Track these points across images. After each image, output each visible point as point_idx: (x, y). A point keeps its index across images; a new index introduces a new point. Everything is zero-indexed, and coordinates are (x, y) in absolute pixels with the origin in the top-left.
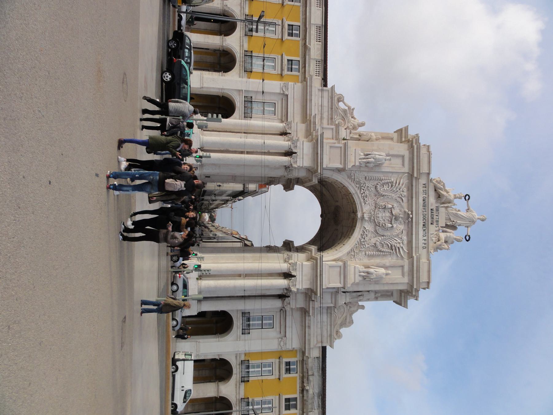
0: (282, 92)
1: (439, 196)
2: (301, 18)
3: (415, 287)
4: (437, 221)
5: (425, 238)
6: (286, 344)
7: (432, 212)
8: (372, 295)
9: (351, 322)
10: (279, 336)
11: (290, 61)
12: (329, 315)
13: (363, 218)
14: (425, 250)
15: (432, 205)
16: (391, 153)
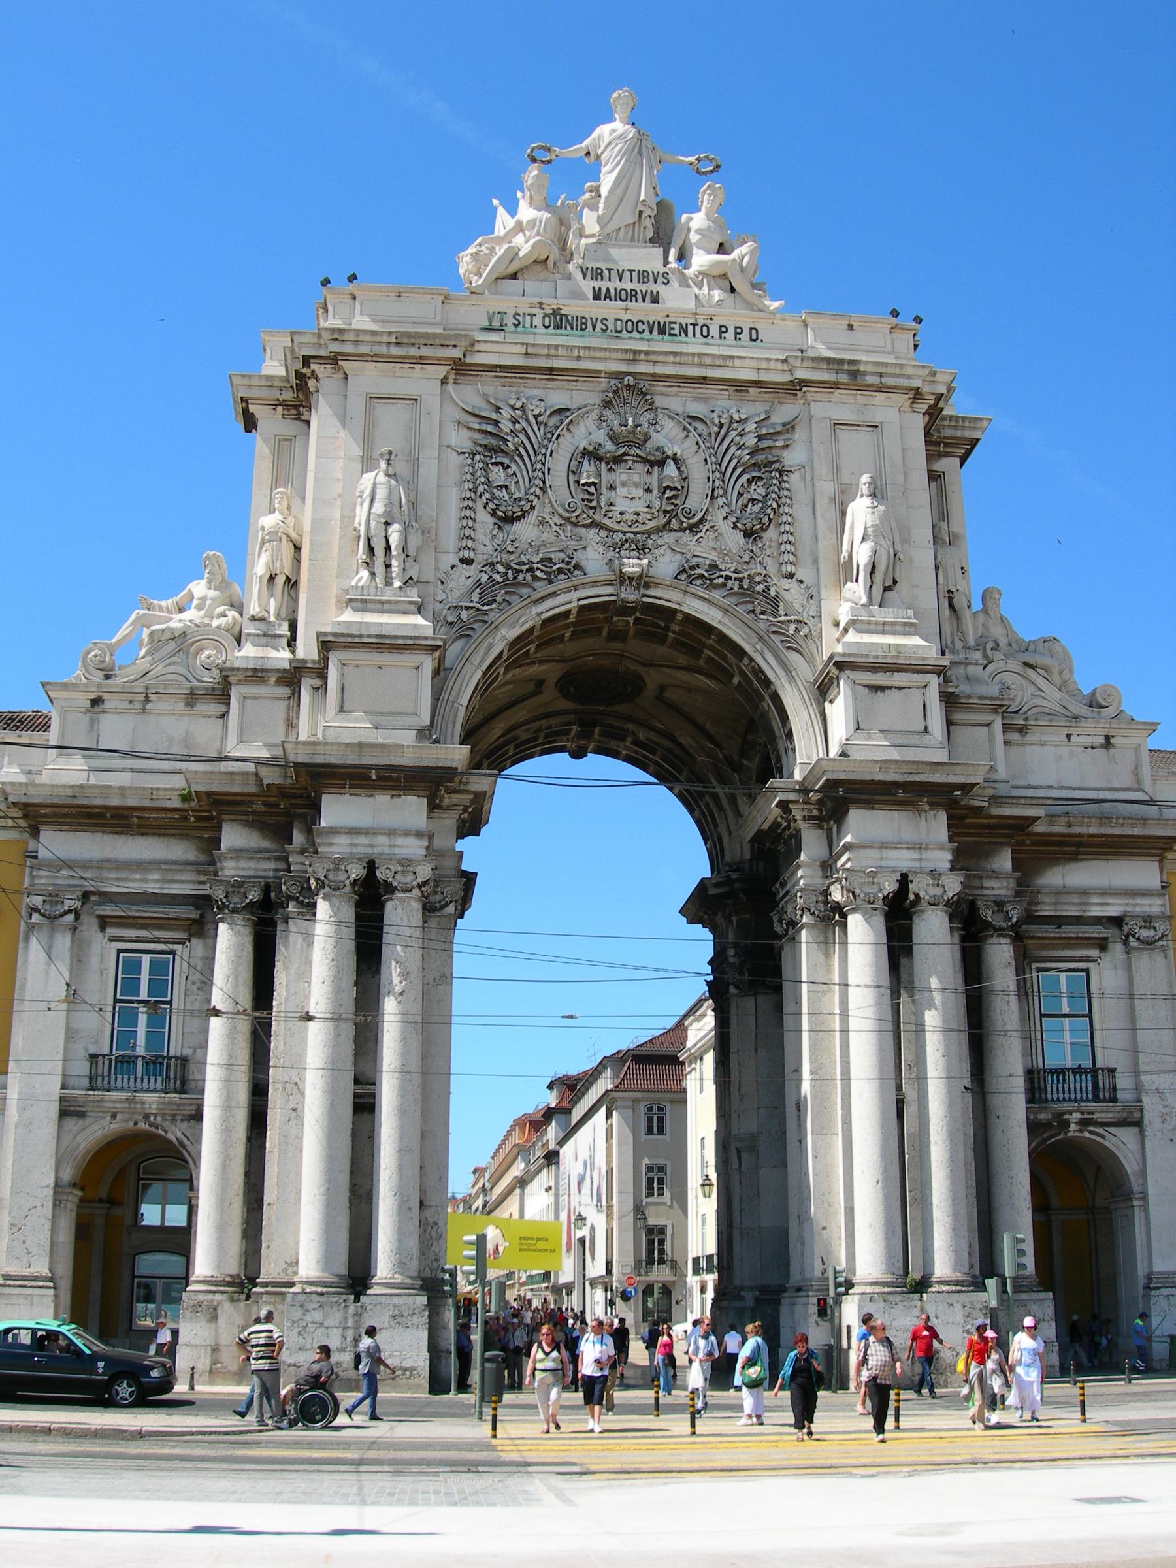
0: (70, 918)
3: (916, 383)
4: (643, 276)
5: (715, 331)
6: (1148, 921)
7: (608, 296)
8: (947, 553)
10: (1117, 948)
13: (642, 581)
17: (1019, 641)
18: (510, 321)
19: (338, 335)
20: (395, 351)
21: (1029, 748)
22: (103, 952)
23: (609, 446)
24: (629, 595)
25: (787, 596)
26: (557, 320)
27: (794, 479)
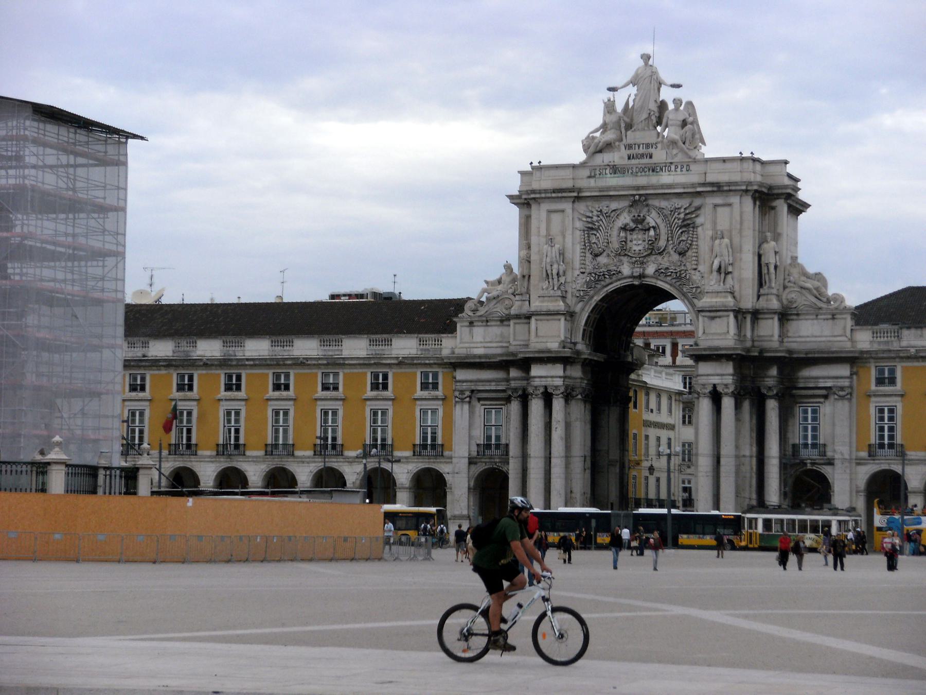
0: (468, 399)
1: (608, 146)
2: (361, 371)
3: (744, 188)
4: (648, 146)
5: (673, 167)
6: (842, 388)
9: (819, 277)
10: (832, 398)
11: (425, 386)
12: (801, 317)
13: (642, 276)
14: (692, 167)
15: (622, 158)
16: (543, 232)
17: (805, 274)
18: (598, 172)
19: (533, 192)
20: (554, 195)
21: (800, 322)
22: (479, 409)
23: (632, 225)
24: (636, 283)
25: (694, 277)
26: (615, 169)
27: (700, 229)
